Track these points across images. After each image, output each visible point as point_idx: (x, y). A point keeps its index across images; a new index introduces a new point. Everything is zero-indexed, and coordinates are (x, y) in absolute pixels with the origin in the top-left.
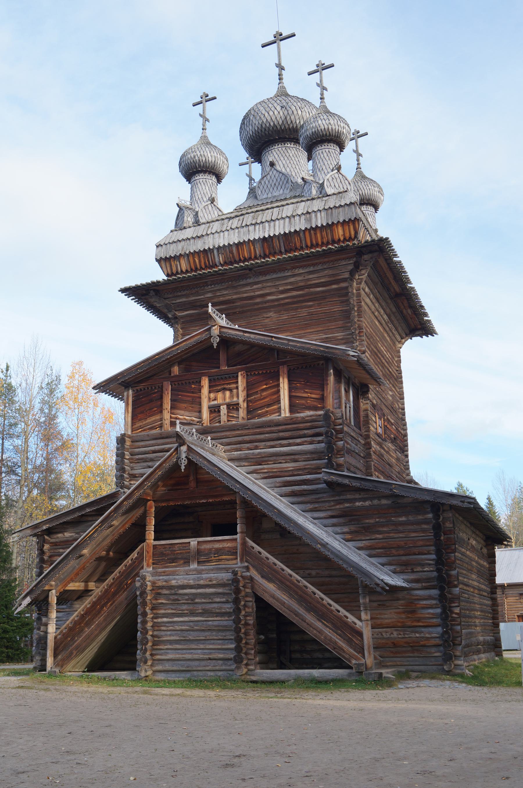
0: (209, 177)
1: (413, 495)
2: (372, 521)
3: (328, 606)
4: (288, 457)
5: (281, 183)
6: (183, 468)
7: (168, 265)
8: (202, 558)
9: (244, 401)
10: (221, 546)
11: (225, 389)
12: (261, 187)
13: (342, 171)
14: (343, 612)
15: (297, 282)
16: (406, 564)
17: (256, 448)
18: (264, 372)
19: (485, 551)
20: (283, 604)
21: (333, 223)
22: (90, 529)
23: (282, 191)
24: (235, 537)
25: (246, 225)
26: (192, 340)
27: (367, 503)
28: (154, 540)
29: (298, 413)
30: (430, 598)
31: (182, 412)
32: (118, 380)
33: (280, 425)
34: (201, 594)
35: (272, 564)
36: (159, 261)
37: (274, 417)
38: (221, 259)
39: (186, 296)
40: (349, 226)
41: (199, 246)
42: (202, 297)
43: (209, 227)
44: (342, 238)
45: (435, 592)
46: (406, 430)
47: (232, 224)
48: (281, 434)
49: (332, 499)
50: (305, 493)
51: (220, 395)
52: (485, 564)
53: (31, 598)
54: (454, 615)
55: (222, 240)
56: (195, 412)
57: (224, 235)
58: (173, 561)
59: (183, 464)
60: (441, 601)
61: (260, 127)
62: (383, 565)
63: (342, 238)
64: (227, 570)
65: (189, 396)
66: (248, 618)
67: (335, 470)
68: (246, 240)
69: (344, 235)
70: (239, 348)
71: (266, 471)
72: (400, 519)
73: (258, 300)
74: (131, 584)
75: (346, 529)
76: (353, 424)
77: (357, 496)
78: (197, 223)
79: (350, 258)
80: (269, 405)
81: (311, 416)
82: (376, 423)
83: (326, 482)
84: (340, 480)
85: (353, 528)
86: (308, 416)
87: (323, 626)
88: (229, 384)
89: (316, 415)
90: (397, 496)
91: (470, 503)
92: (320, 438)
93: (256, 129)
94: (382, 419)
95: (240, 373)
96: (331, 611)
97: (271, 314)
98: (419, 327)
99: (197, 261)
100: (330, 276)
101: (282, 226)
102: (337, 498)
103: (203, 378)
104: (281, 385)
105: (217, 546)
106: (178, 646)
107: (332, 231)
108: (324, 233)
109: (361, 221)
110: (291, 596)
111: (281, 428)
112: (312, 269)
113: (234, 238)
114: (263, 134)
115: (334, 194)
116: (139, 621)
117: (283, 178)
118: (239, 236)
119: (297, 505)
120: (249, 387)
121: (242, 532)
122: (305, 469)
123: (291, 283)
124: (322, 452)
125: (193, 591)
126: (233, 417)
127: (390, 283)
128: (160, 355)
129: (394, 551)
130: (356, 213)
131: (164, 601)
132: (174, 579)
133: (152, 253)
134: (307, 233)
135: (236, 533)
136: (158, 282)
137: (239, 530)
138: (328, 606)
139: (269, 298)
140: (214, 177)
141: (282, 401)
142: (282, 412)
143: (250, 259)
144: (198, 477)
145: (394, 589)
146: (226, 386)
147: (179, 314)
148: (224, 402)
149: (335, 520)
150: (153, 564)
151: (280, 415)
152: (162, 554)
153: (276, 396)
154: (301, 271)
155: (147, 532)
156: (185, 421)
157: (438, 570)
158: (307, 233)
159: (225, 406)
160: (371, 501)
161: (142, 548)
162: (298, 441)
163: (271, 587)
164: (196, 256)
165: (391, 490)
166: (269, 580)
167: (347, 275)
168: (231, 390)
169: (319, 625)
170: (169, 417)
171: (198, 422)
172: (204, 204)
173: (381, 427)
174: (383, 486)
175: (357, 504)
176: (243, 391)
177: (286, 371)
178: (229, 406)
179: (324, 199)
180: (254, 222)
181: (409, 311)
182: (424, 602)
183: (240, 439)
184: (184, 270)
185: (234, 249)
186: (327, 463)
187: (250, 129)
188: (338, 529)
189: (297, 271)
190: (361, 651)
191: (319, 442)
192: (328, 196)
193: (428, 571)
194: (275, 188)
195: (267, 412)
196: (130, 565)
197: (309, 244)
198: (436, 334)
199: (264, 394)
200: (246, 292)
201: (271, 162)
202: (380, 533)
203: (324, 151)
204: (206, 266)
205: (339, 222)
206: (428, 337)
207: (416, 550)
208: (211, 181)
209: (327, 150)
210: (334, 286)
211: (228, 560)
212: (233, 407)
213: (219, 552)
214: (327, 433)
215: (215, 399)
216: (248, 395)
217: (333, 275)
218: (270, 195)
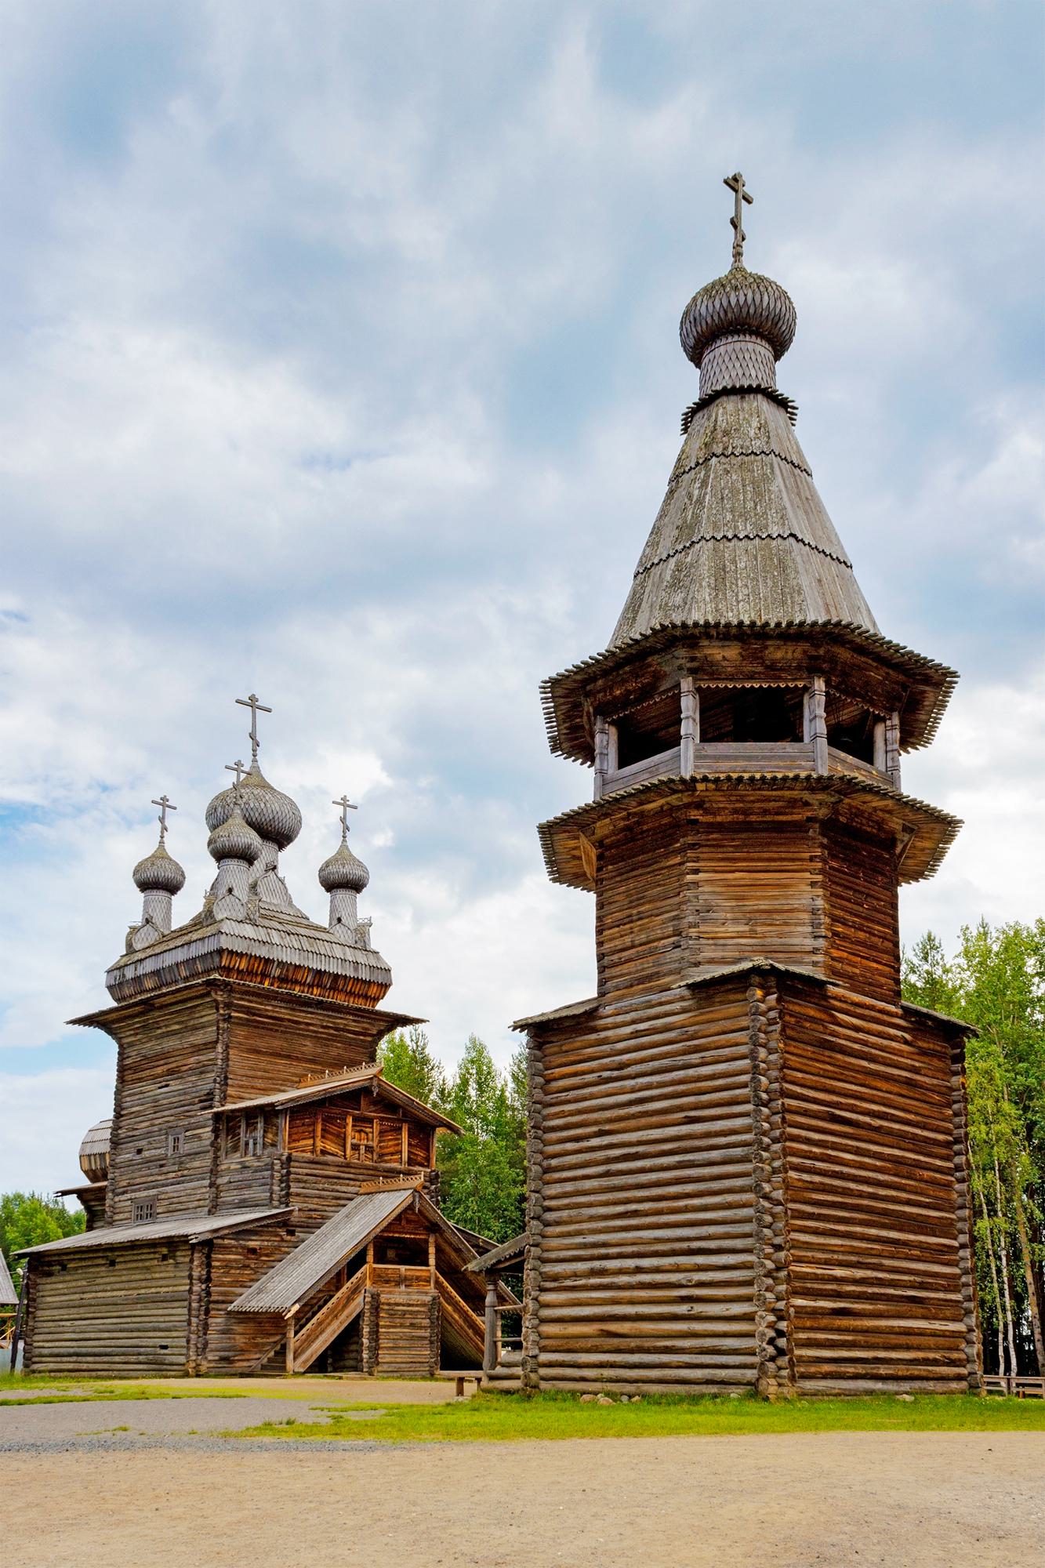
8: (408, 1283)
15: (338, 1024)
28: (374, 1263)
31: (329, 1143)
39: (251, 1002)
41: (263, 952)
58: (387, 1282)
80: (392, 1154)
99: (256, 965)
100: (363, 1028)
105: (418, 1274)
106: (392, 1352)
118: (299, 959)
123: (333, 1023)
125: (405, 1308)
139: (311, 1028)
152: (380, 1276)
153: (396, 1148)
154: (351, 1017)
163: (450, 1308)
168: (367, 1134)
178: (366, 1146)
185: (291, 969)
189: (348, 1017)
199: (390, 1143)
210: (362, 1037)
213: (418, 1279)
216: (380, 1142)
217: (366, 1029)
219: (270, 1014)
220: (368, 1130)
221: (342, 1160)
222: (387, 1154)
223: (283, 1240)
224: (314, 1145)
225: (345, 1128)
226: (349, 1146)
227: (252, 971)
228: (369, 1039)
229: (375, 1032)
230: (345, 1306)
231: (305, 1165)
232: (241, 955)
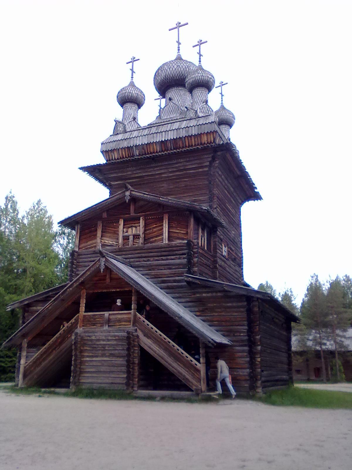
0: (133, 105)
1: (235, 291)
2: (212, 305)
3: (181, 354)
4: (166, 267)
5: (175, 110)
6: (102, 270)
7: (107, 154)
10: (122, 317)
11: (132, 227)
12: (164, 113)
14: (190, 358)
16: (230, 331)
18: (155, 217)
19: (284, 325)
20: (155, 352)
21: (201, 133)
22: (47, 304)
23: (175, 114)
24: (130, 311)
25: (152, 133)
27: (209, 295)
28: (85, 312)
29: (174, 241)
30: (243, 351)
31: (108, 239)
33: (162, 248)
34: (109, 345)
35: (150, 328)
36: (102, 152)
37: (159, 244)
40: (210, 135)
41: (125, 144)
42: (126, 174)
43: (131, 134)
44: (206, 142)
45: (246, 348)
46: (242, 254)
47: (144, 132)
49: (190, 291)
50: (175, 287)
51: (130, 230)
52: (285, 333)
54: (257, 363)
55: (139, 142)
56: (115, 239)
57: (139, 139)
59: (102, 268)
60: (249, 354)
61: (164, 77)
62: (217, 331)
63: (206, 142)
64: (124, 331)
65: (111, 230)
66: (135, 360)
67: (192, 275)
68: (152, 142)
69: (207, 140)
70: (142, 203)
71: (153, 274)
72: (228, 305)
74: (70, 337)
75: (196, 309)
76: (206, 249)
77: (204, 290)
78: (125, 132)
79: (210, 154)
80: (157, 236)
81: (180, 243)
82: (222, 249)
83: (186, 281)
84: (194, 281)
85: (201, 309)
86: (178, 243)
87: (178, 366)
88: (135, 224)
89: (183, 243)
90: (227, 291)
91: (269, 297)
92: (185, 256)
93: (162, 78)
94: (227, 247)
95: (141, 218)
96: (183, 357)
97: (163, 185)
98: (253, 195)
101: (172, 135)
102: (193, 291)
103: (121, 220)
104: (164, 225)
107: (201, 138)
108: (196, 139)
109: (218, 132)
110: (160, 347)
111: (163, 249)
112: (188, 159)
113: (145, 141)
114: (166, 81)
115: (203, 117)
116: (73, 359)
117: (176, 108)
119: (169, 294)
120: (146, 226)
121: (134, 309)
122: (175, 273)
124: (185, 264)
126: (136, 242)
127: (234, 169)
128: (97, 206)
129: (224, 323)
130: (215, 128)
131: (87, 348)
133: (99, 147)
134: (186, 138)
135: (131, 310)
136: (100, 164)
137: (132, 308)
138: (181, 354)
139: (163, 175)
140: (136, 105)
141: (164, 234)
143: (154, 153)
144: (111, 276)
145: (220, 346)
146: (133, 225)
147: (113, 183)
148: (132, 234)
149: (190, 304)
151: (163, 242)
153: (160, 231)
154: (182, 161)
155: (80, 307)
157: (248, 336)
158: (186, 138)
159: (132, 236)
160: (212, 293)
161: (78, 316)
162: (172, 257)
164: (123, 150)
165: (223, 287)
166: (149, 337)
167: (208, 164)
168: (136, 227)
169: (175, 365)
170: (100, 241)
171: (116, 245)
172: (130, 121)
173: (225, 252)
174: (218, 285)
175: (204, 295)
177: (167, 217)
178: (134, 236)
179: (197, 119)
180: (156, 132)
181: (246, 186)
182: (240, 354)
183: (139, 255)
184: (116, 158)
186: (187, 271)
187: (159, 79)
188: (193, 309)
190: (199, 380)
191: (184, 258)
192: (199, 117)
193: (243, 336)
194: (172, 113)
195: (156, 240)
196: (71, 326)
197: (187, 145)
198: (262, 199)
199: (155, 230)
201: (170, 98)
202: (217, 312)
203: (199, 91)
205: (204, 133)
207: (237, 323)
208: (134, 108)
209: (201, 91)
210: (200, 170)
211: (125, 325)
212: (136, 237)
214: (188, 253)
215: (127, 232)
216: (145, 230)
217: (200, 163)
218: (168, 117)
219: (133, 176)
222: (152, 238)
228: (206, 169)
229: (208, 164)
230: (61, 343)
232: (112, 151)
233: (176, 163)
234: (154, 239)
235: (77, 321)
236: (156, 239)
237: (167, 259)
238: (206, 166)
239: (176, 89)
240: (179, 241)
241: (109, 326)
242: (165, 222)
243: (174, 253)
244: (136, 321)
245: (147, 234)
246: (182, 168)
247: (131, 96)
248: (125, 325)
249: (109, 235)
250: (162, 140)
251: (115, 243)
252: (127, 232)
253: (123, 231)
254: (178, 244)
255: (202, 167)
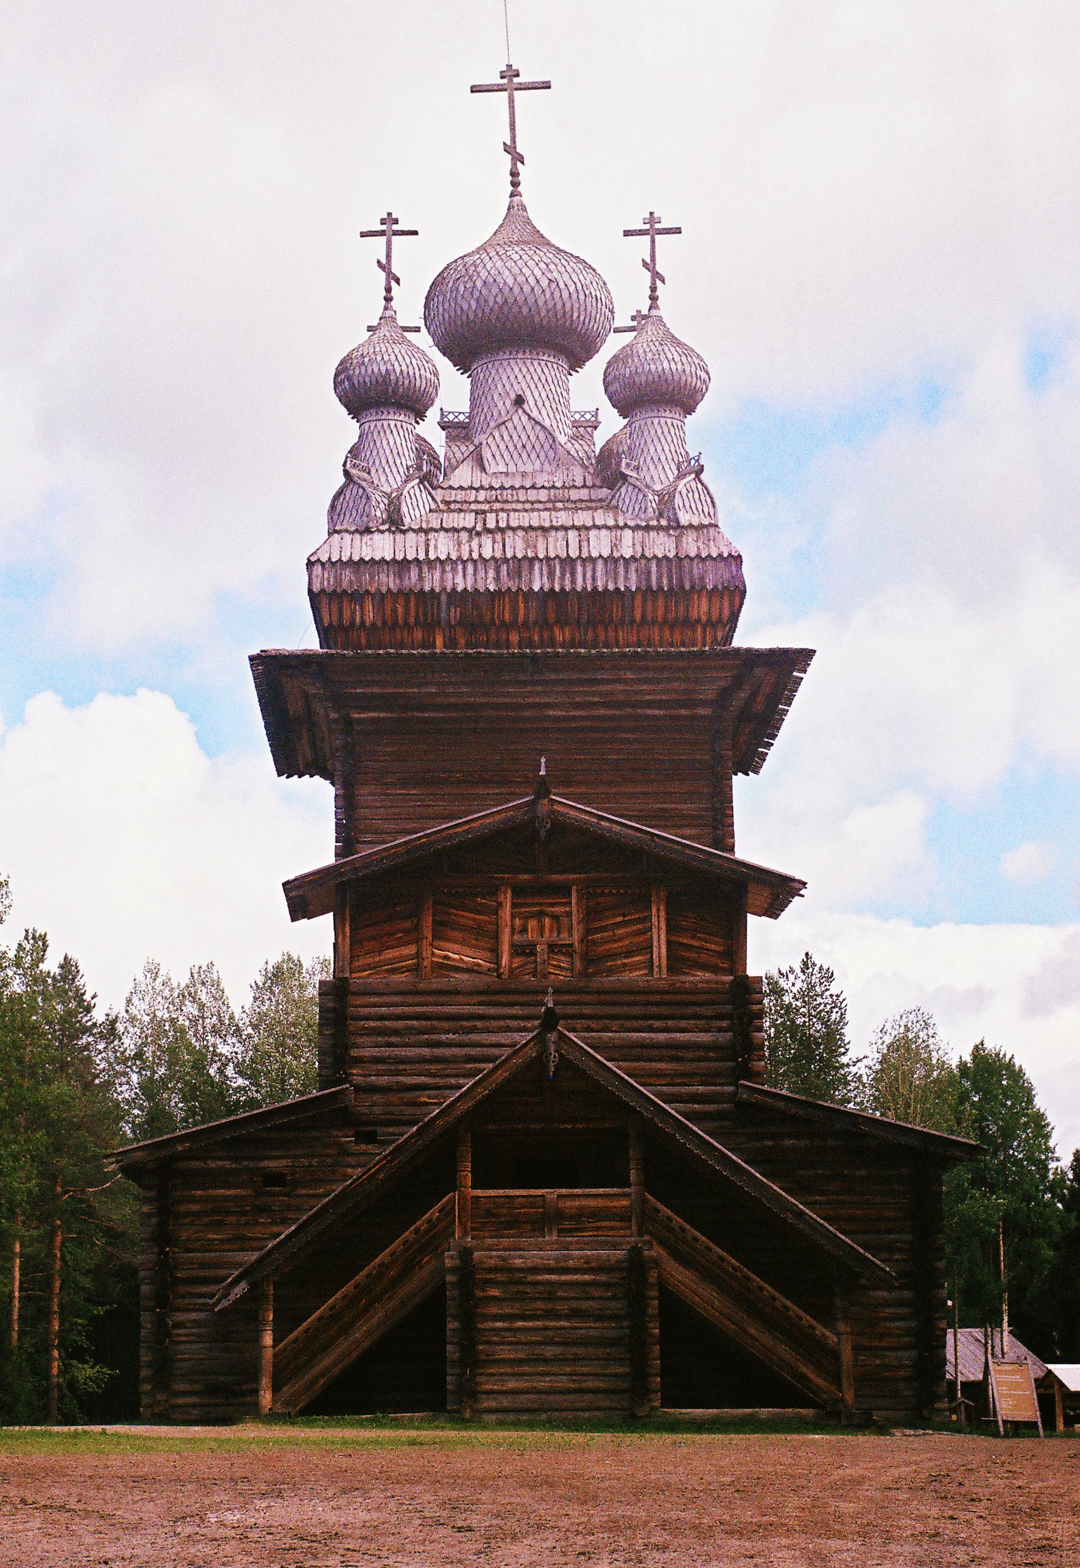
7: (334, 608)
8: (567, 1225)
9: (582, 941)
13: (702, 476)
14: (807, 1319)
17: (605, 1029)
26: (497, 818)
28: (473, 1187)
30: (901, 1303)
31: (456, 947)
32: (341, 874)
38: (452, 614)
45: (906, 1294)
48: (654, 1010)
53: (250, 1284)
54: (938, 1332)
55: (461, 582)
56: (484, 949)
58: (509, 1225)
63: (704, 618)
73: (528, 713)
80: (629, 954)
81: (707, 982)
88: (553, 905)
92: (725, 1024)
95: (574, 889)
99: (400, 610)
104: (654, 920)
105: (593, 1203)
118: (497, 579)
120: (591, 915)
123: (601, 694)
125: (554, 1277)
132: (521, 1257)
142: (656, 969)
150: (473, 1229)
156: (465, 966)
159: (545, 947)
162: (683, 1024)
164: (401, 601)
168: (555, 918)
171: (489, 970)
176: (579, 923)
190: (836, 1379)
191: (720, 1030)
197: (638, 616)
199: (621, 931)
200: (508, 695)
204: (417, 622)
206: (748, 775)
210: (683, 712)
211: (612, 1228)
213: (596, 1215)
216: (588, 932)
219: (439, 700)
220: (557, 910)
221: (492, 979)
223: (347, 1153)
224: (418, 955)
225: (497, 913)
226: (505, 948)
227: (396, 623)
230: (396, 1282)
231: (397, 999)
233: (609, 682)
234: (619, 962)
235: (447, 1212)
236: (626, 961)
237: (666, 1030)
238: (704, 703)
239: (527, 355)
240: (701, 976)
241: (560, 1231)
242: (658, 910)
243: (690, 1010)
244: (646, 1220)
245: (594, 942)
246: (621, 697)
247: (408, 388)
248: (612, 1228)
249: (458, 935)
250: (552, 590)
251: (480, 961)
252: (524, 930)
253: (513, 928)
254: (700, 985)
255: (692, 704)
